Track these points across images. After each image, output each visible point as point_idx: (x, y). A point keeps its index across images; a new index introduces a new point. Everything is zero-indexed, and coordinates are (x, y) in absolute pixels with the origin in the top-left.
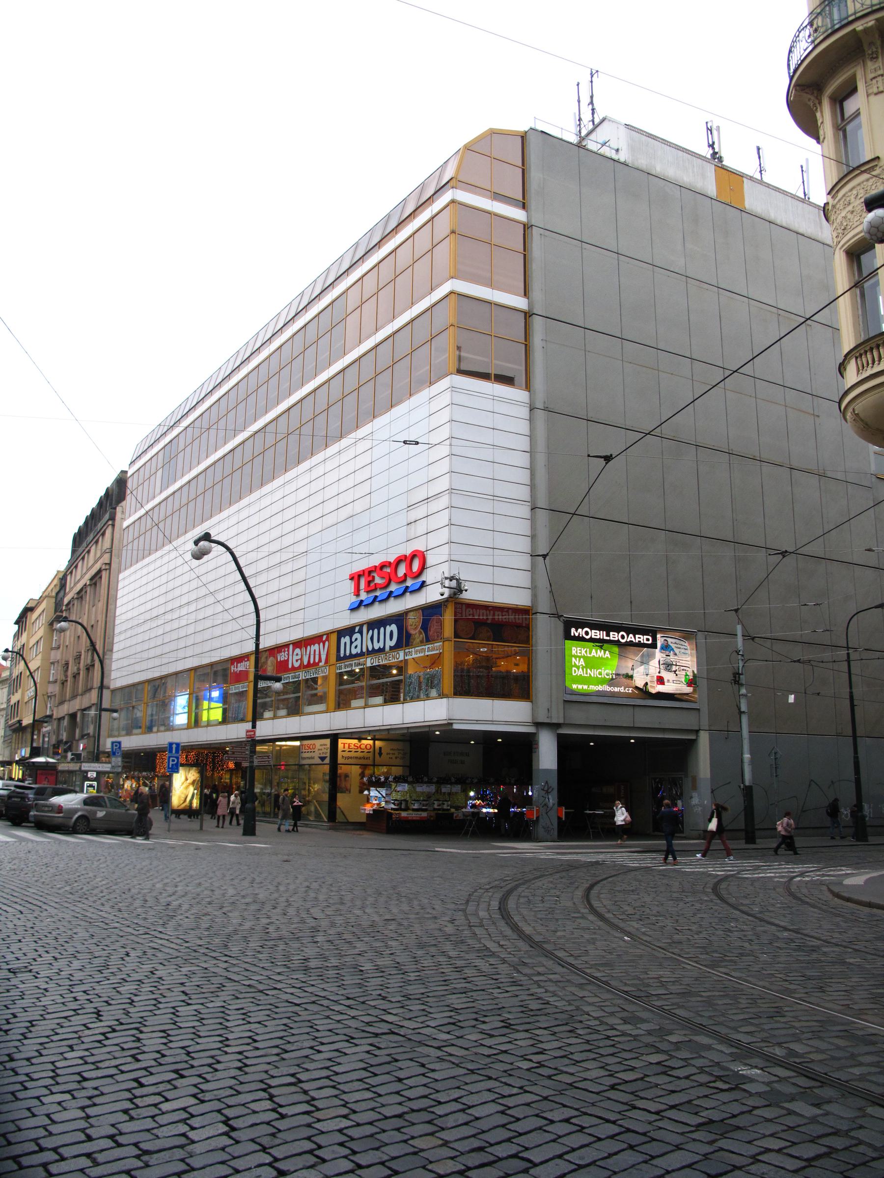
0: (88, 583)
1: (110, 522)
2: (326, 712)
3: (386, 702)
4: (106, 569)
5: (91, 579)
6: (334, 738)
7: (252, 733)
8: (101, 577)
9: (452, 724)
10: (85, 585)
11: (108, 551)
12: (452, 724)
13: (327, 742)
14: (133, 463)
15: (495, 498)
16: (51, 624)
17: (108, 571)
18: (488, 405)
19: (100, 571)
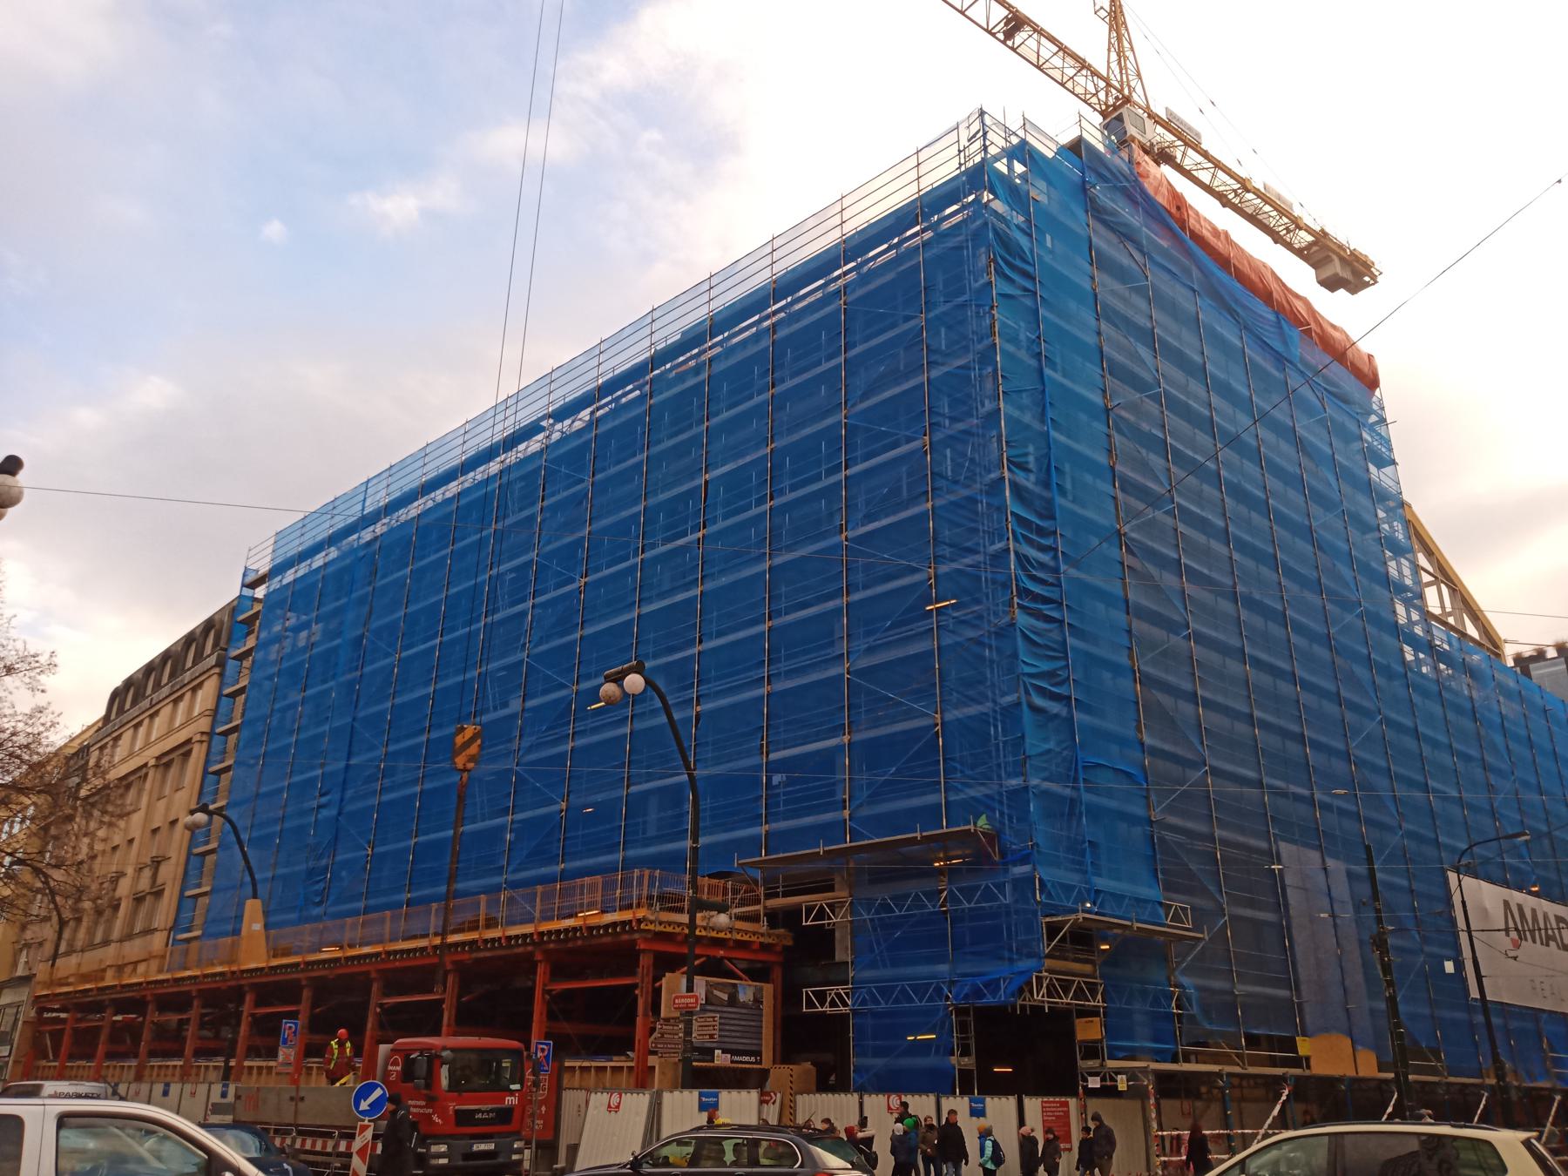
0: (152, 762)
1: (217, 670)
4: (201, 742)
5: (158, 758)
7: (693, 1000)
8: (187, 754)
10: (145, 765)
11: (207, 713)
16: (46, 829)
17: (205, 745)
19: (189, 741)
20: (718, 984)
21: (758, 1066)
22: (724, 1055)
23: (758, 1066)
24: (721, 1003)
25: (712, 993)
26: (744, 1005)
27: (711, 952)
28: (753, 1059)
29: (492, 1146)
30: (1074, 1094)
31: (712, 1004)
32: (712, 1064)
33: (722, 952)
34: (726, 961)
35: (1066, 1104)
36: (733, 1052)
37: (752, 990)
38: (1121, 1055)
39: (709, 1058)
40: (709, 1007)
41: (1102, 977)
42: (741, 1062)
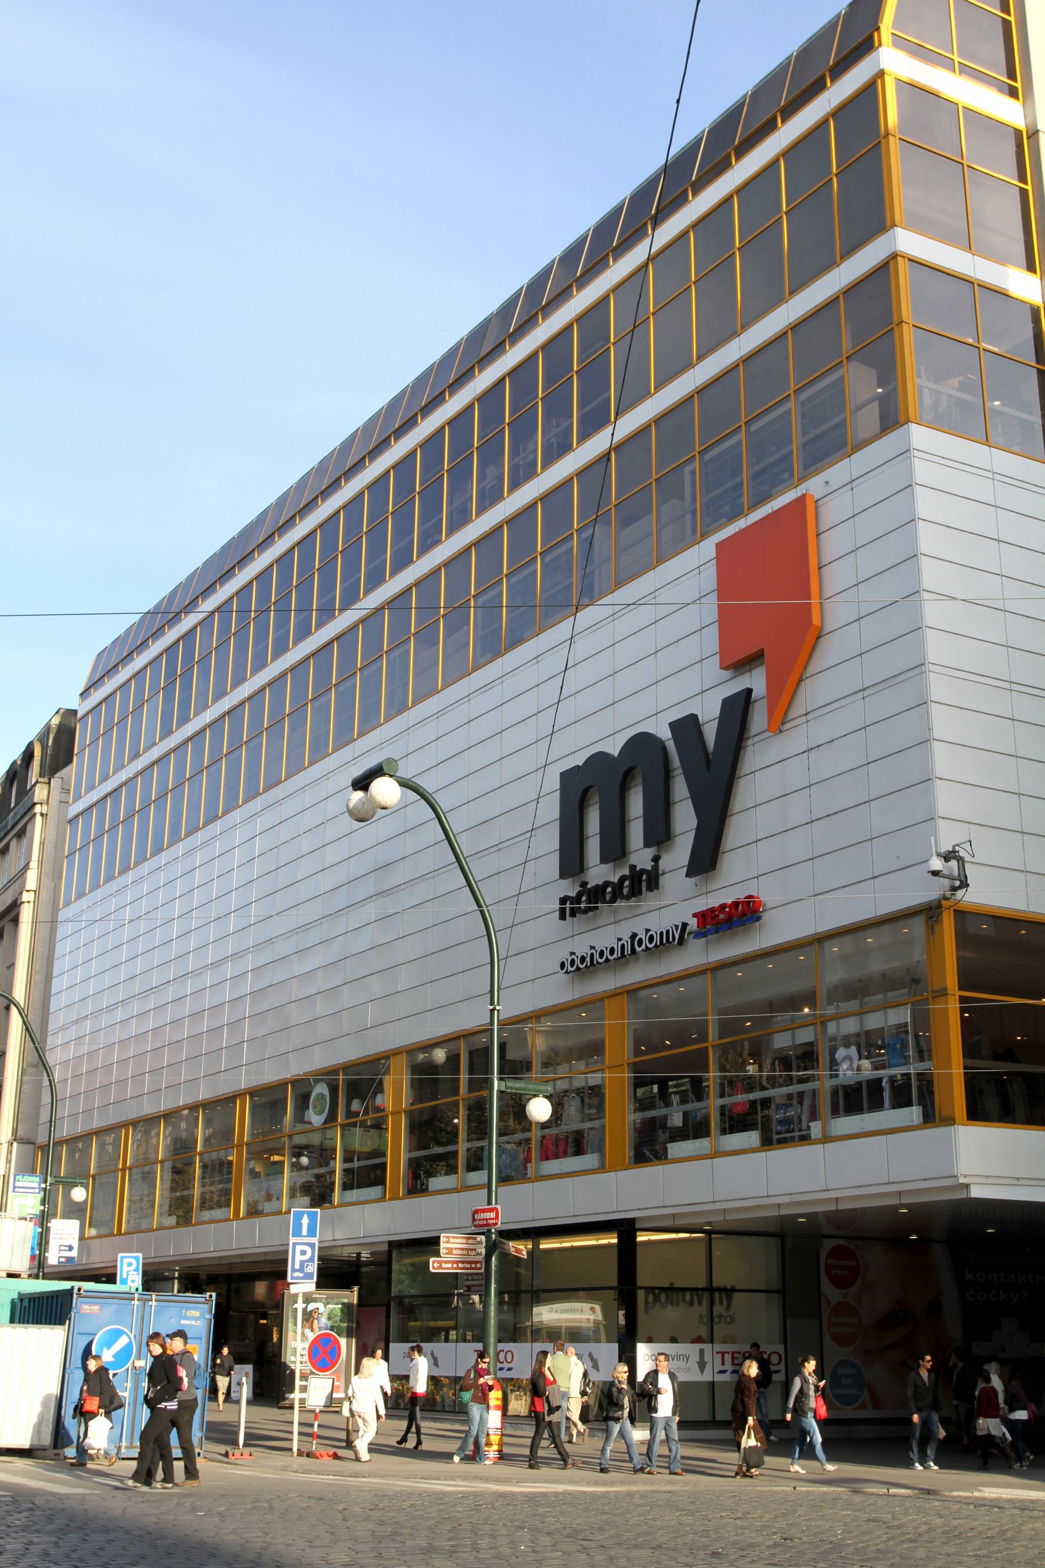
2: (602, 1168)
3: (767, 1142)
6: (626, 1229)
7: (492, 1215)
9: (967, 1186)
12: (967, 1186)
13: (611, 1239)
14: (84, 694)
15: (1014, 687)
18: (982, 489)
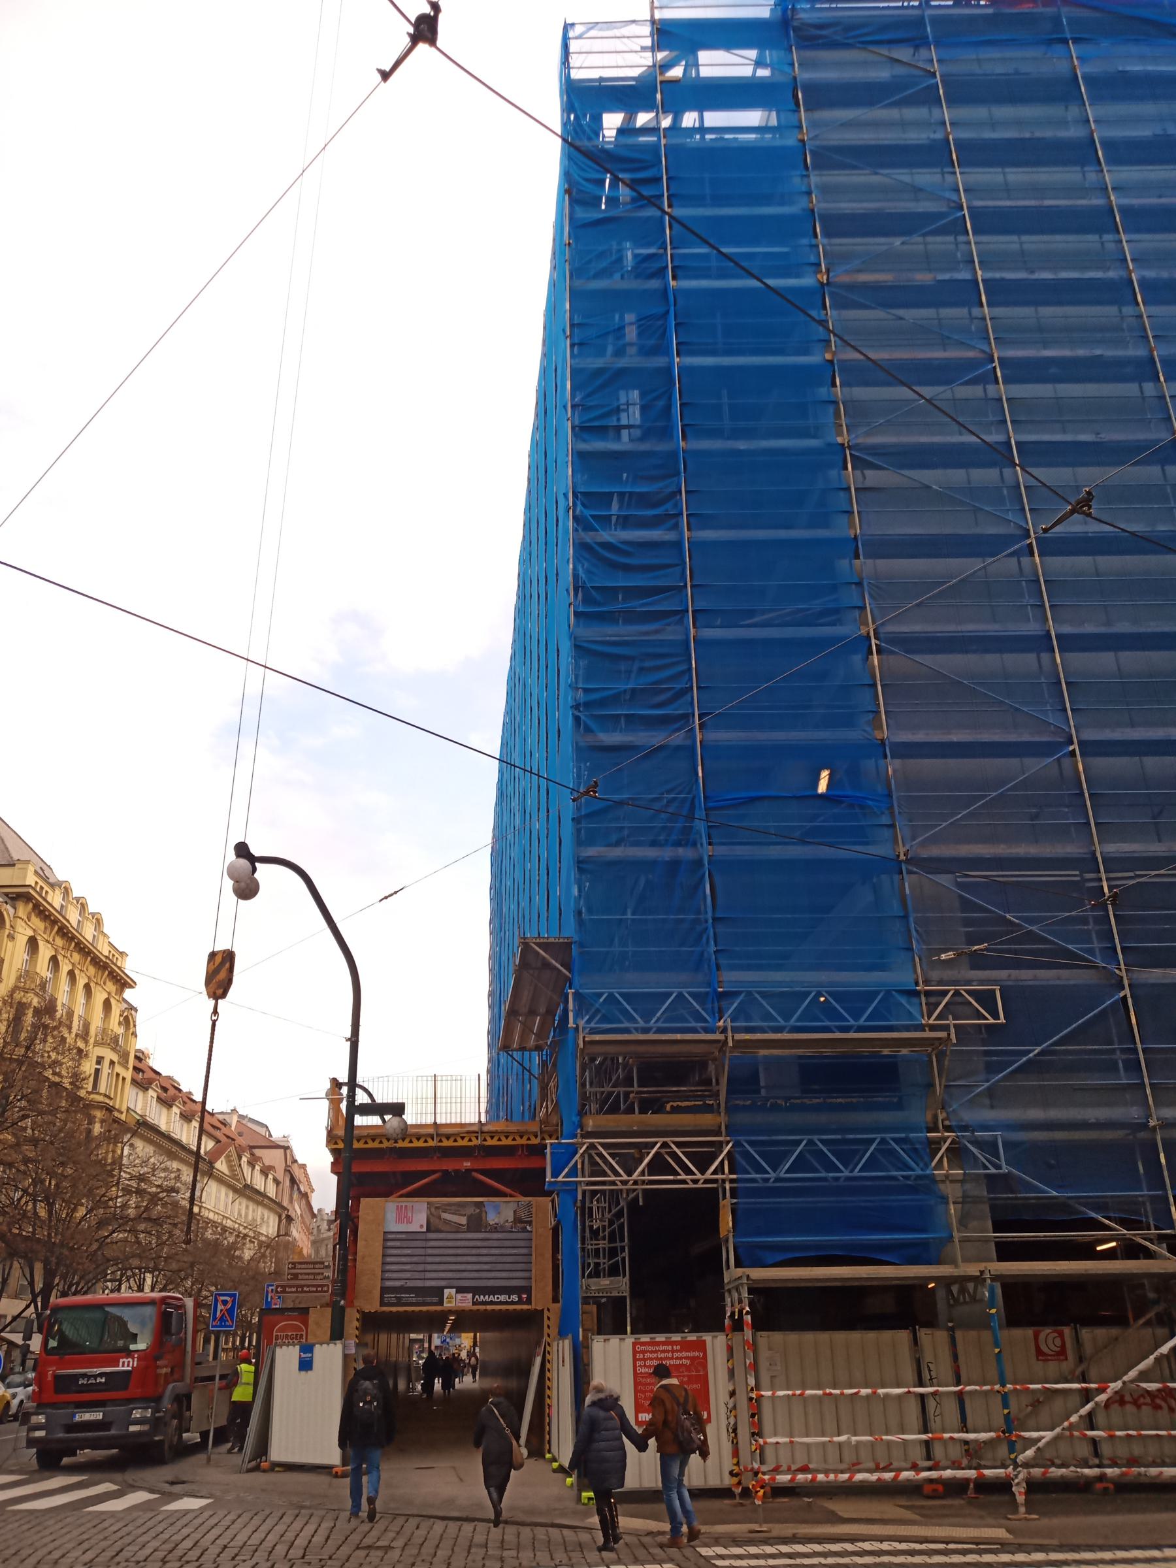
20: (450, 1204)
21: (525, 1307)
22: (459, 1296)
23: (525, 1307)
24: (457, 1228)
25: (439, 1217)
26: (495, 1229)
27: (450, 1165)
28: (514, 1298)
29: (100, 1416)
30: (720, 1328)
31: (438, 1231)
32: (439, 1308)
33: (467, 1164)
34: (475, 1174)
35: (701, 1346)
36: (475, 1291)
37: (513, 1206)
38: (770, 1257)
39: (435, 1300)
40: (431, 1235)
41: (730, 1131)
42: (492, 1303)
